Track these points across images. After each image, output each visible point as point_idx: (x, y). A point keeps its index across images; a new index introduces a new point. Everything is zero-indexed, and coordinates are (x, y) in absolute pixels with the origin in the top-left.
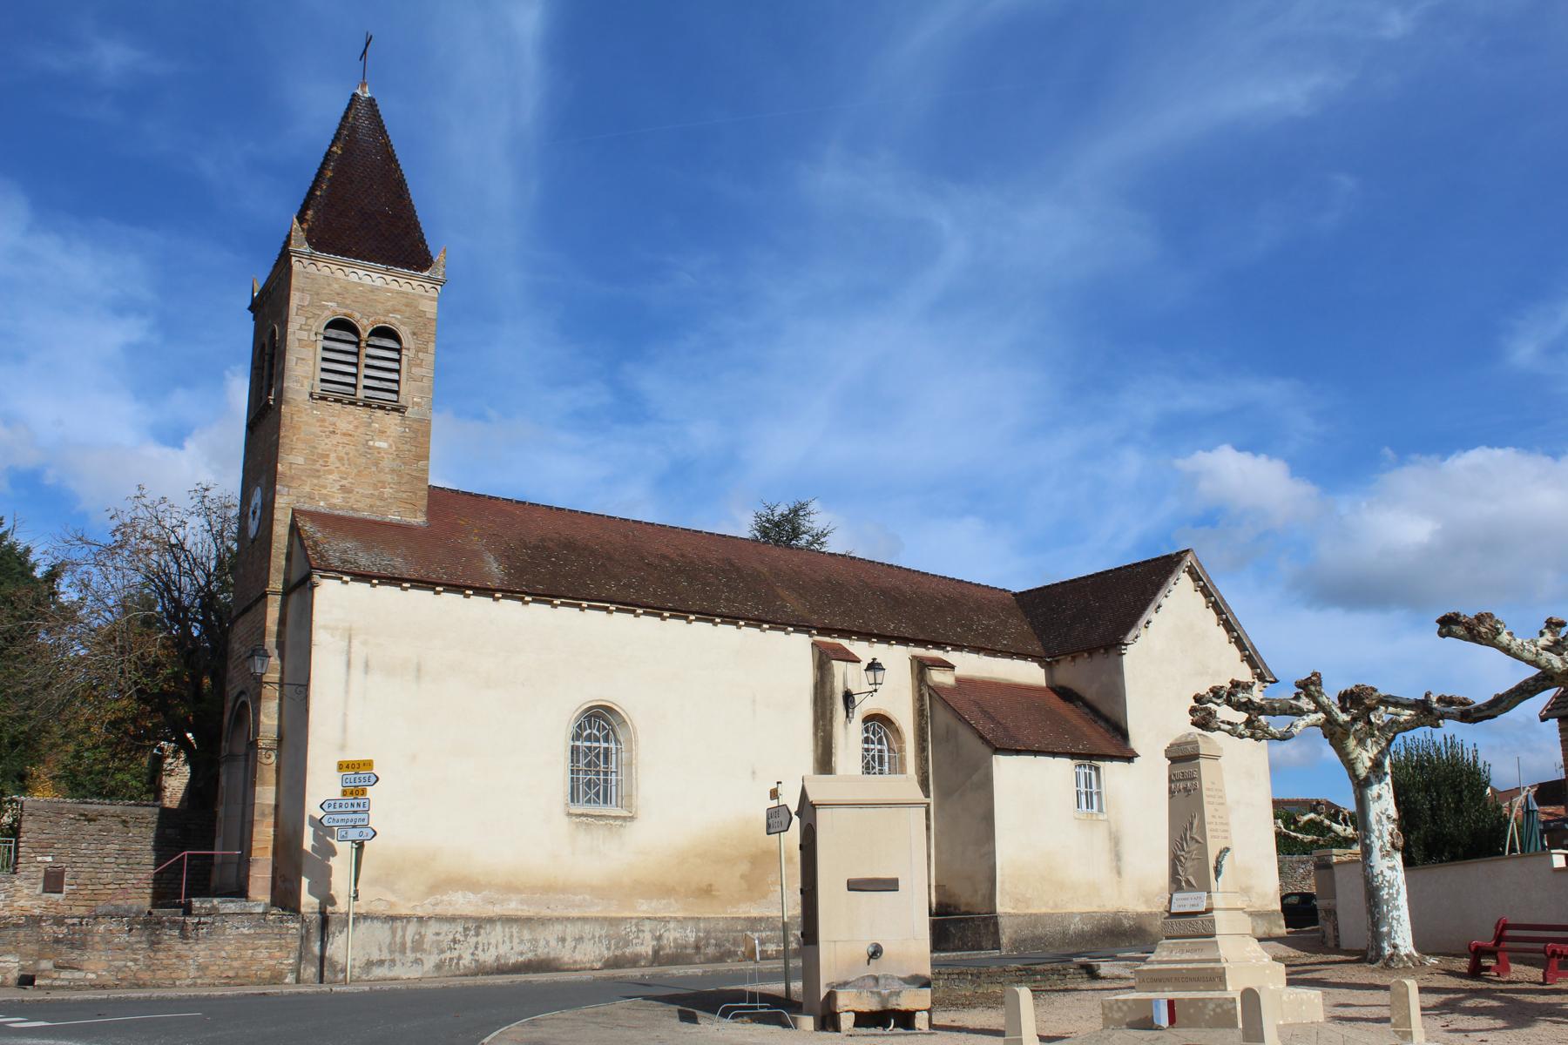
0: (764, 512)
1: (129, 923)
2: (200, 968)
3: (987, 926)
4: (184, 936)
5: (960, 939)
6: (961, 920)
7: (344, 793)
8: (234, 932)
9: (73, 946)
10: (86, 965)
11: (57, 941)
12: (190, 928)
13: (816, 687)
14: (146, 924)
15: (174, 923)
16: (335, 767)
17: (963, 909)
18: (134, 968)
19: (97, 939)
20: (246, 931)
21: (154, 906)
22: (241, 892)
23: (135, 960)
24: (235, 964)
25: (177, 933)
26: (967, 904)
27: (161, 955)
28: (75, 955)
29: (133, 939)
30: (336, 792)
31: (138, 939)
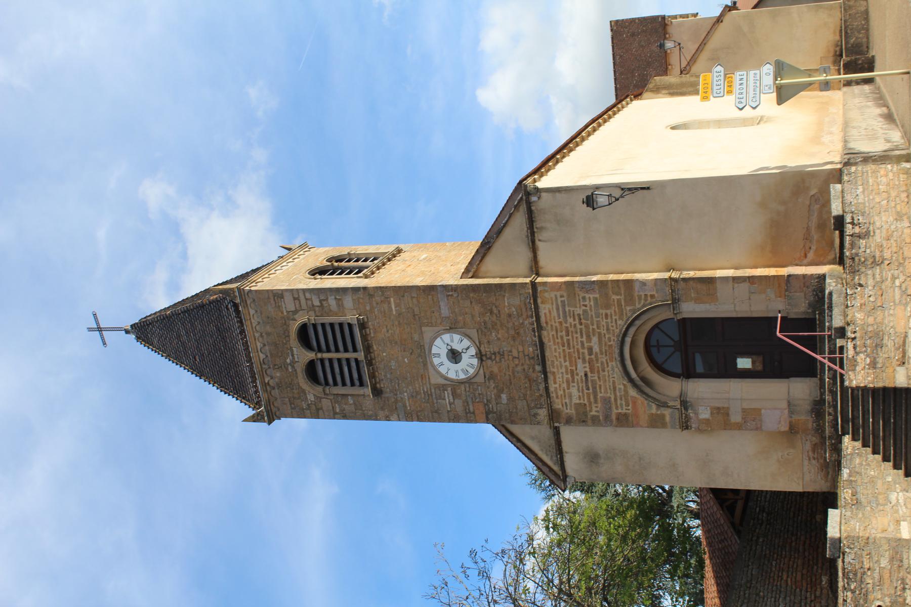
0: (528, 479)
1: (855, 287)
2: (899, 217)
3: (850, 7)
4: (866, 235)
5: (859, 32)
6: (846, 32)
7: (730, 92)
8: (861, 197)
9: (879, 346)
10: (900, 329)
11: (873, 365)
12: (857, 230)
13: (672, 94)
14: (854, 272)
15: (853, 245)
16: (706, 103)
17: (838, 38)
18: (902, 278)
19: (871, 320)
20: (860, 189)
21: (835, 329)
22: (822, 278)
23: (894, 278)
24: (893, 194)
25: (862, 242)
26: (834, 33)
27: (887, 255)
28: (889, 343)
29: (871, 282)
30: (730, 100)
31: (869, 278)
